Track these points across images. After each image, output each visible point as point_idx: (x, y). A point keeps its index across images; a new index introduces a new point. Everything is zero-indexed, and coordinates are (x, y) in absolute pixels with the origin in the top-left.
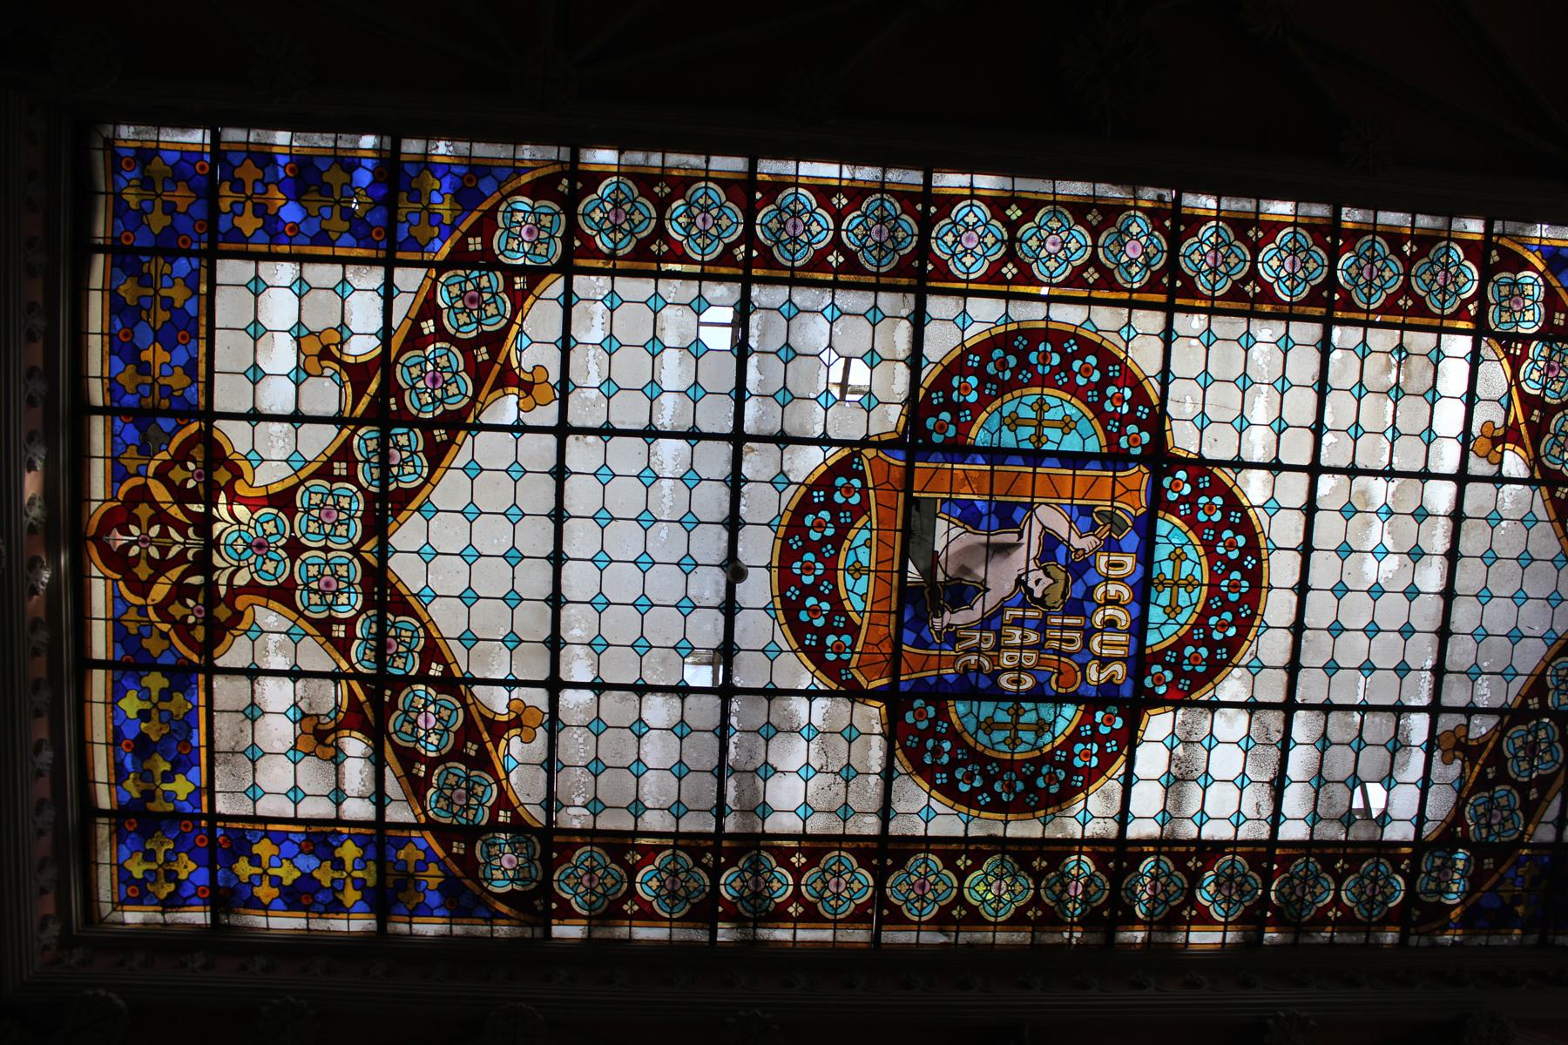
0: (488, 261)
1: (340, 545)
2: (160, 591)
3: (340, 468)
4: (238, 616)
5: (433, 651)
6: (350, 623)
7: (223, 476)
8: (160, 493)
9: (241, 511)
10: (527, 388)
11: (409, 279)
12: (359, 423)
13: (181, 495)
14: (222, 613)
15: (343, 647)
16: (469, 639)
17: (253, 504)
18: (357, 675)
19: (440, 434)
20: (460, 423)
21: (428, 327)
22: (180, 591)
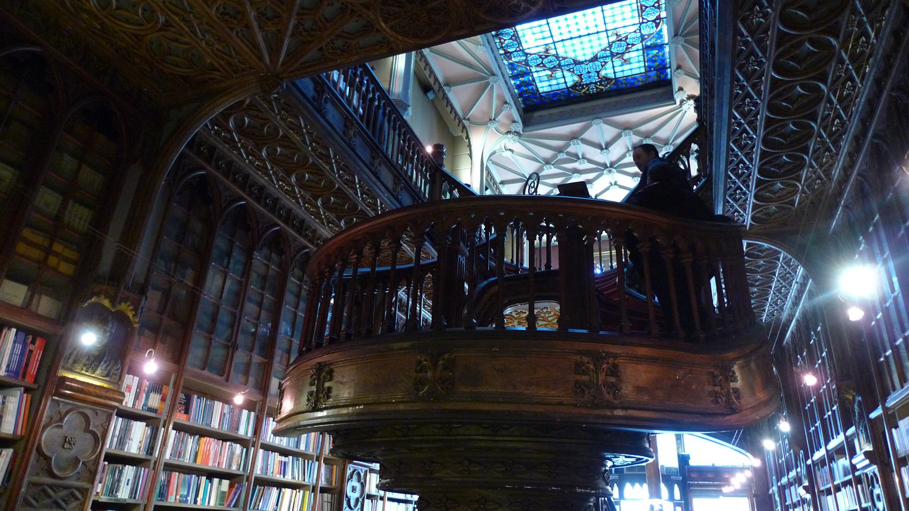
0: (526, 61)
1: (586, 67)
2: (601, 87)
3: (571, 70)
4: (604, 77)
5: (605, 50)
6: (601, 62)
7: (578, 84)
8: (584, 91)
9: (583, 81)
10: (547, 50)
11: (533, 69)
12: (562, 70)
13: (583, 88)
14: (604, 79)
15: (606, 63)
16: (600, 45)
17: (582, 79)
18: (612, 60)
19: (561, 59)
20: (557, 56)
21: (541, 65)
22: (601, 85)
